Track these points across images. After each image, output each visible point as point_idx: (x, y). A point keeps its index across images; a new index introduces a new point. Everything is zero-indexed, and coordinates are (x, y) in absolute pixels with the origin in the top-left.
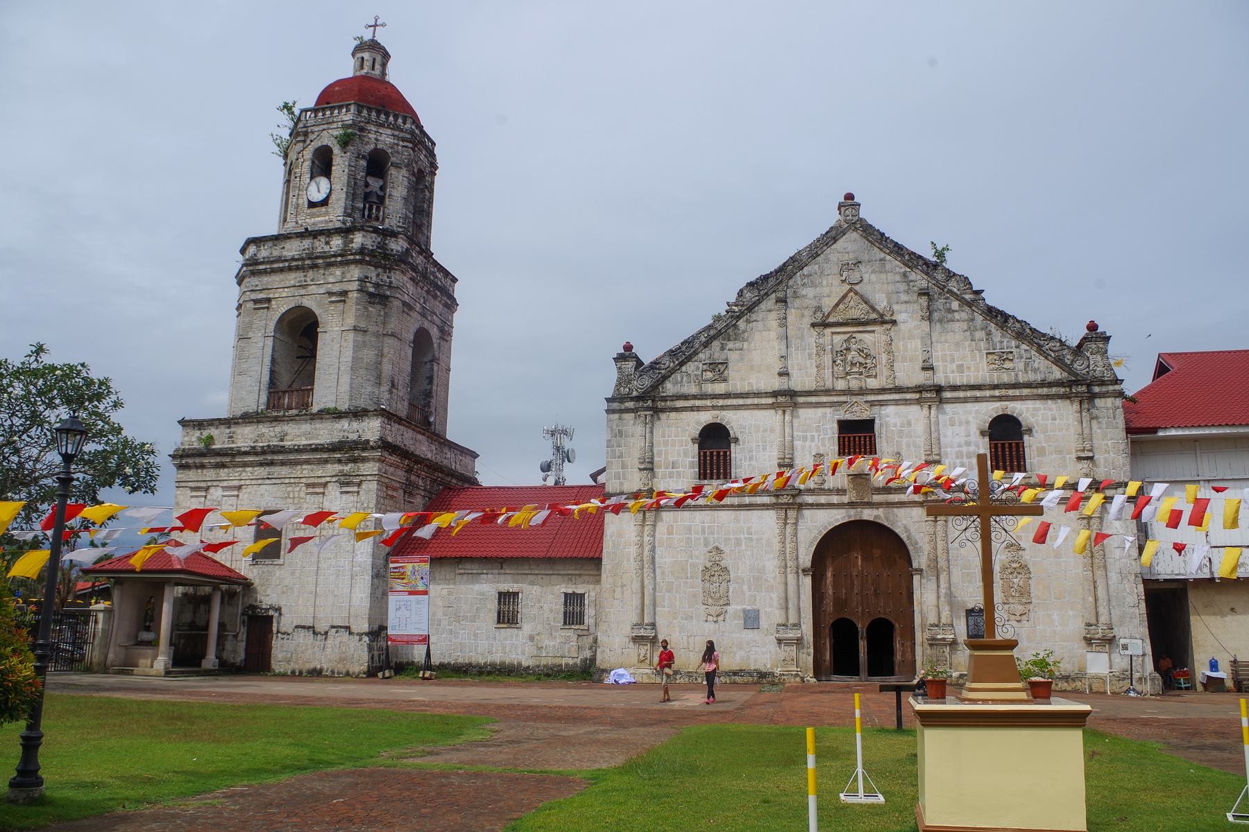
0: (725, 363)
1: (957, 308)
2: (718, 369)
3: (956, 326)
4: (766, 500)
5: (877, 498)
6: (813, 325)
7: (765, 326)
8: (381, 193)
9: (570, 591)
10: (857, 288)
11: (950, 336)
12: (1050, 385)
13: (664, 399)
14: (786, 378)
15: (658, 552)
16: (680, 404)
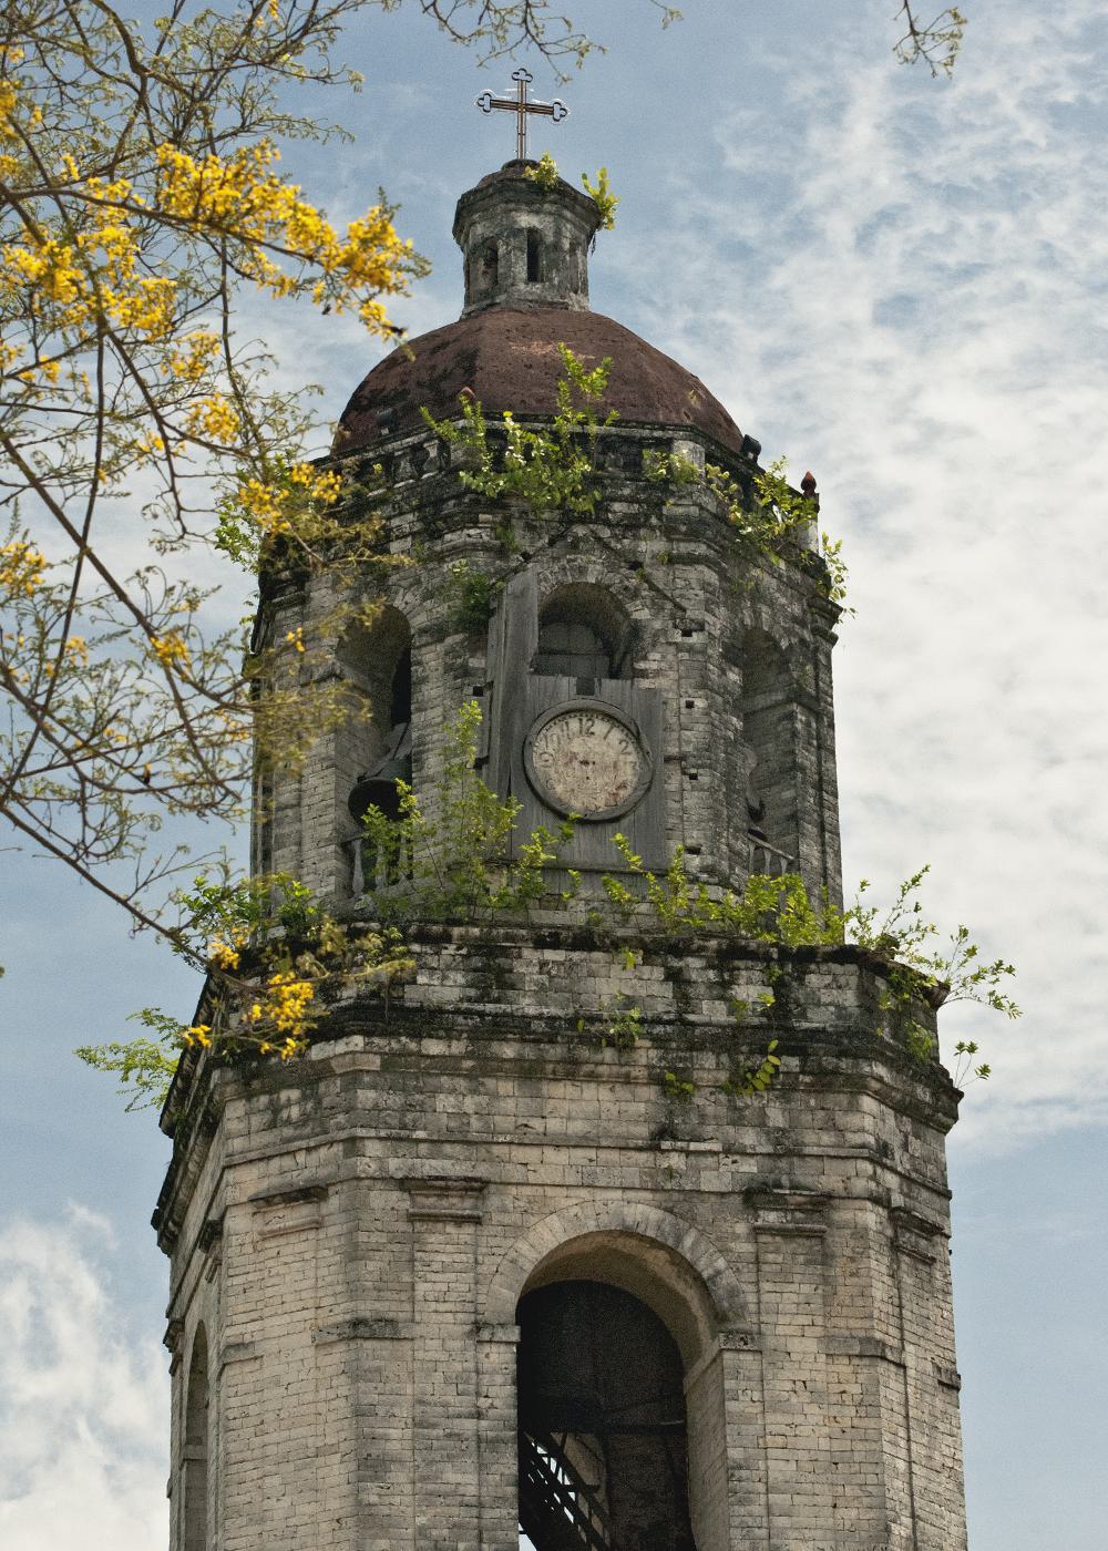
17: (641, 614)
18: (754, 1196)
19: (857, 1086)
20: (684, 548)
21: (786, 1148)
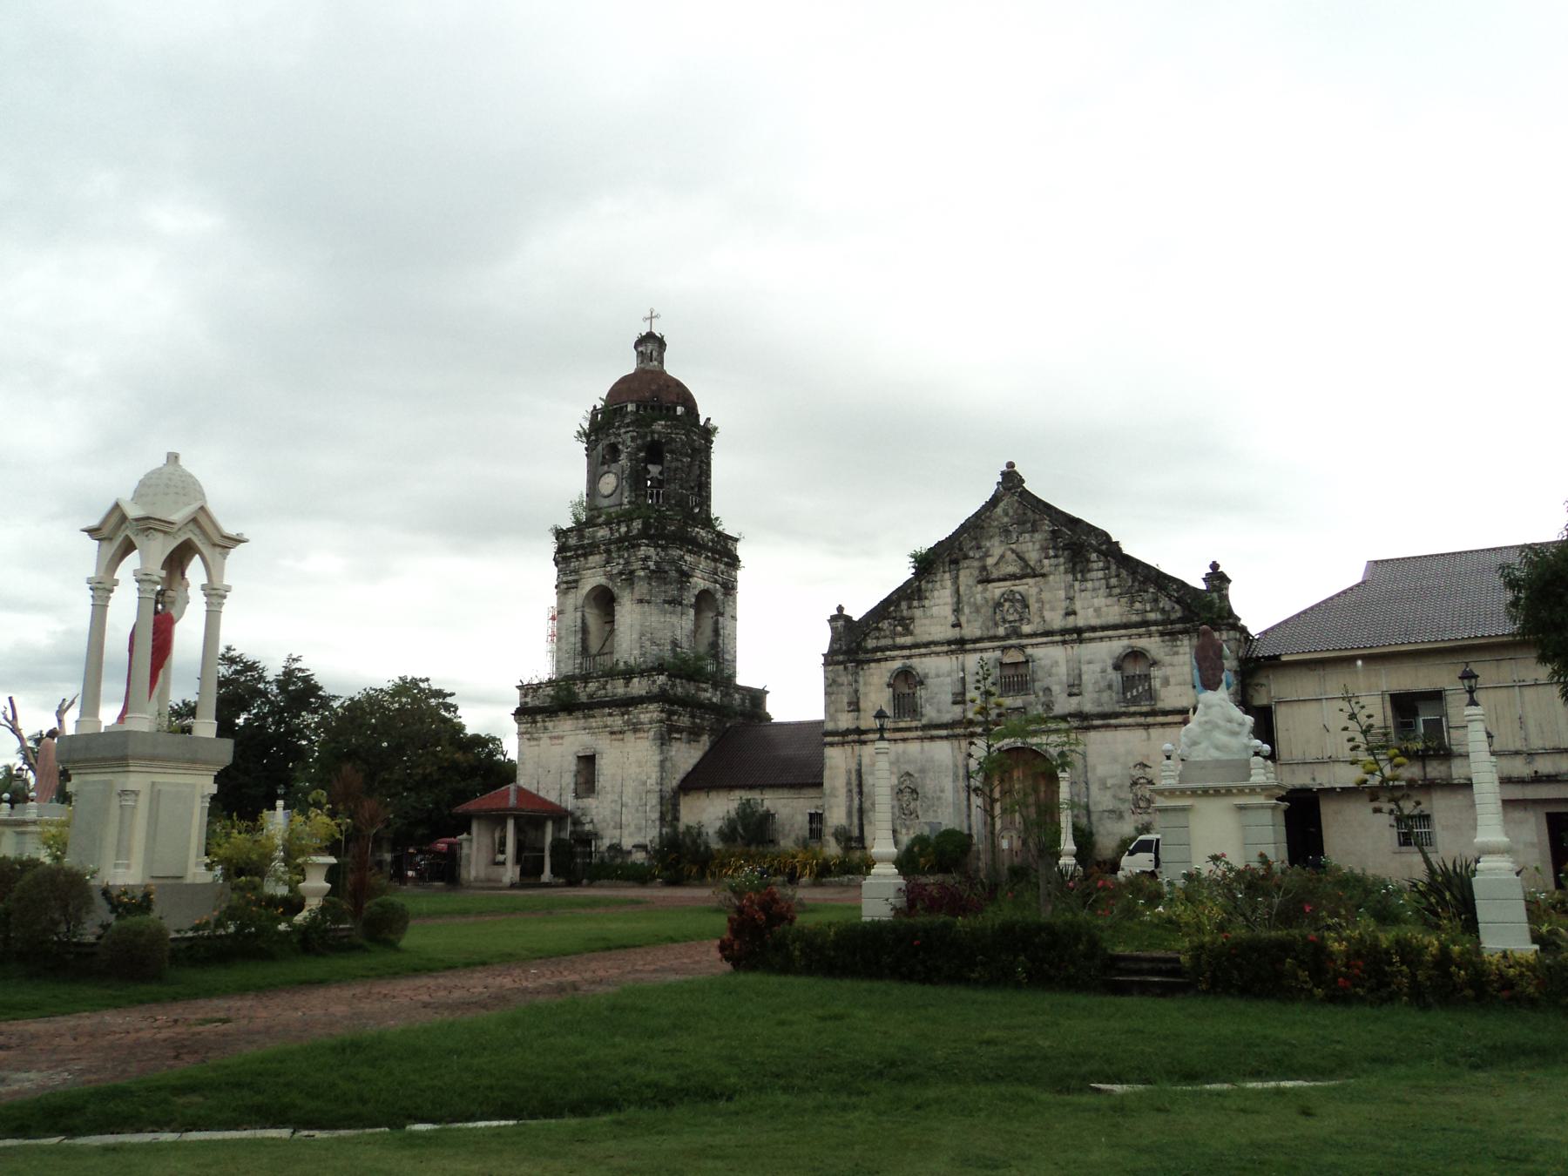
0: (912, 619)
1: (1096, 559)
2: (906, 625)
3: (1094, 575)
4: (944, 733)
5: (1032, 727)
6: (980, 582)
7: (941, 585)
8: (660, 477)
9: (813, 811)
10: (1014, 546)
11: (1089, 585)
12: (1172, 623)
13: (867, 651)
14: (958, 629)
15: (864, 777)
16: (879, 655)
17: (620, 447)
18: (621, 573)
19: (640, 546)
20: (628, 429)
21: (627, 563)
